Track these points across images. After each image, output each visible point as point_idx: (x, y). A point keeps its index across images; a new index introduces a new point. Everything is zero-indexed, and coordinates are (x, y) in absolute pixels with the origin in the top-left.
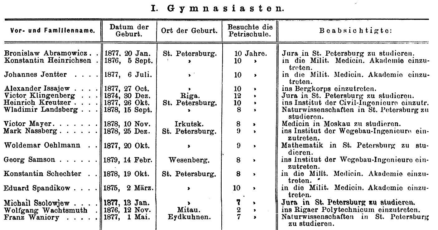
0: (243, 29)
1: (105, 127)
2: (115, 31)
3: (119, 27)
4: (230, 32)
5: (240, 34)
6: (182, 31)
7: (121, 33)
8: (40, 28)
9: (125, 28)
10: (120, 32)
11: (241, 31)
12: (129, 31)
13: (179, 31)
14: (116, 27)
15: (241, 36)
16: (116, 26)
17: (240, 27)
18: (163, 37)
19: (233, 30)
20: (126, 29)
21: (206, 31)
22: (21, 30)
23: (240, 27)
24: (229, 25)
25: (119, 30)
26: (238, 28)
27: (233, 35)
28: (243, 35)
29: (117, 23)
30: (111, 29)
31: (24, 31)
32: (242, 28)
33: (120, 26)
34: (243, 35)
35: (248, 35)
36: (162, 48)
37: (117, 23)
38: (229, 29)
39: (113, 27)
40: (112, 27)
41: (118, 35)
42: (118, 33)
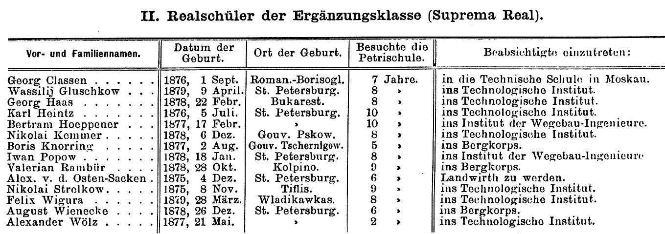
1: (166, 119)
2: (182, 53)
3: (189, 48)
7: (190, 57)
9: (197, 48)
12: (203, 54)
14: (183, 48)
20: (198, 50)
22: (40, 53)
25: (188, 52)
29: (184, 43)
31: (43, 54)
37: (184, 43)
39: (178, 49)
42: (186, 57)
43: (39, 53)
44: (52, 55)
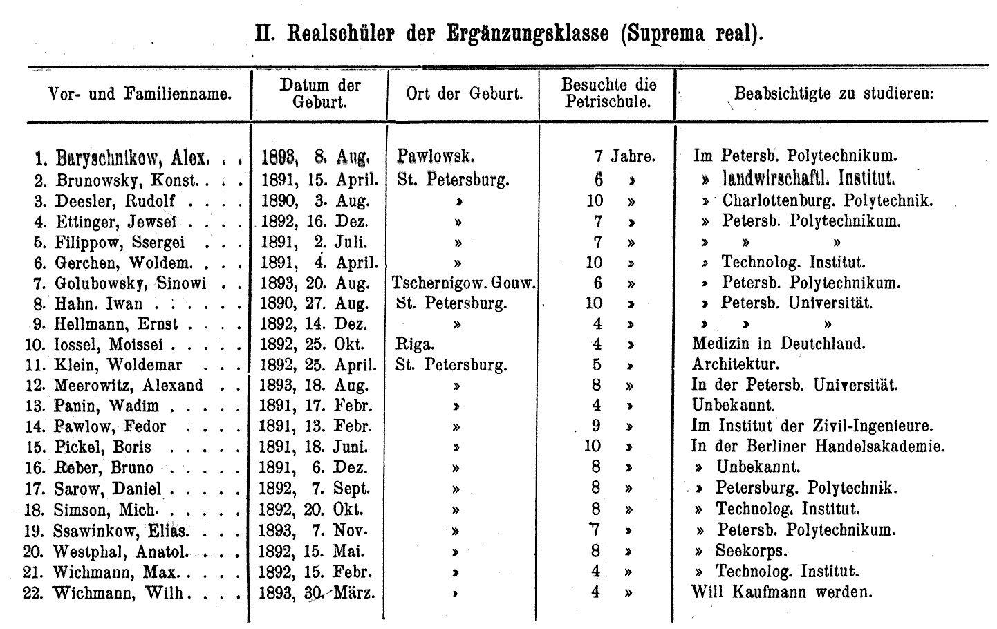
0: (595, 89)
2: (292, 93)
3: (302, 86)
4: (569, 96)
5: (589, 102)
6: (450, 94)
7: (305, 100)
8: (112, 88)
10: (302, 97)
11: (592, 95)
13: (445, 94)
14: (294, 86)
15: (592, 106)
16: (296, 84)
17: (588, 85)
18: (402, 108)
19: (573, 91)
21: (505, 95)
22: (73, 92)
23: (588, 85)
24: (565, 79)
26: (584, 86)
27: (574, 104)
28: (596, 103)
30: (284, 89)
31: (79, 95)
32: (593, 86)
33: (305, 83)
34: (596, 103)
35: (606, 103)
36: (403, 137)
37: (297, 76)
38: (565, 89)
40: (286, 85)
41: (298, 104)
42: (298, 99)
43: (71, 92)
44: (93, 95)
